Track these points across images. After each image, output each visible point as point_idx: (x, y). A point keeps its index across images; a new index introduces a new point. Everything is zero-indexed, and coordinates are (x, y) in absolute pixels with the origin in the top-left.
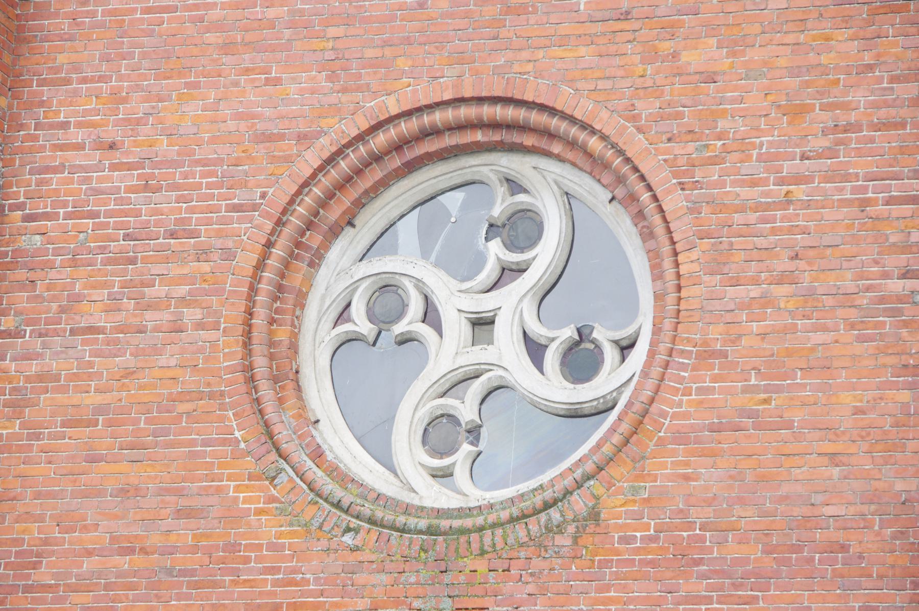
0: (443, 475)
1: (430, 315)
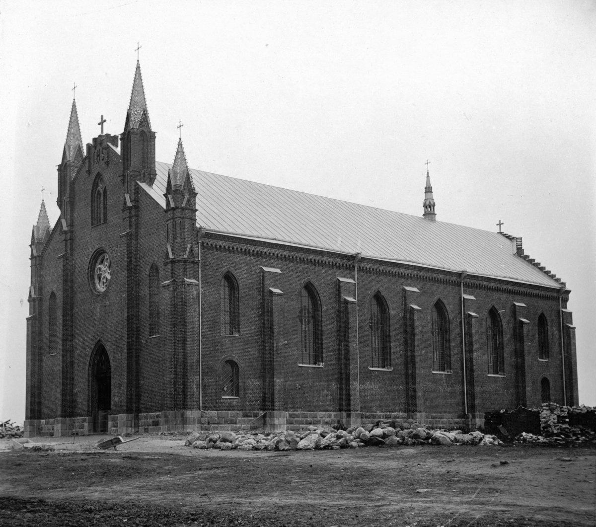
0: (103, 288)
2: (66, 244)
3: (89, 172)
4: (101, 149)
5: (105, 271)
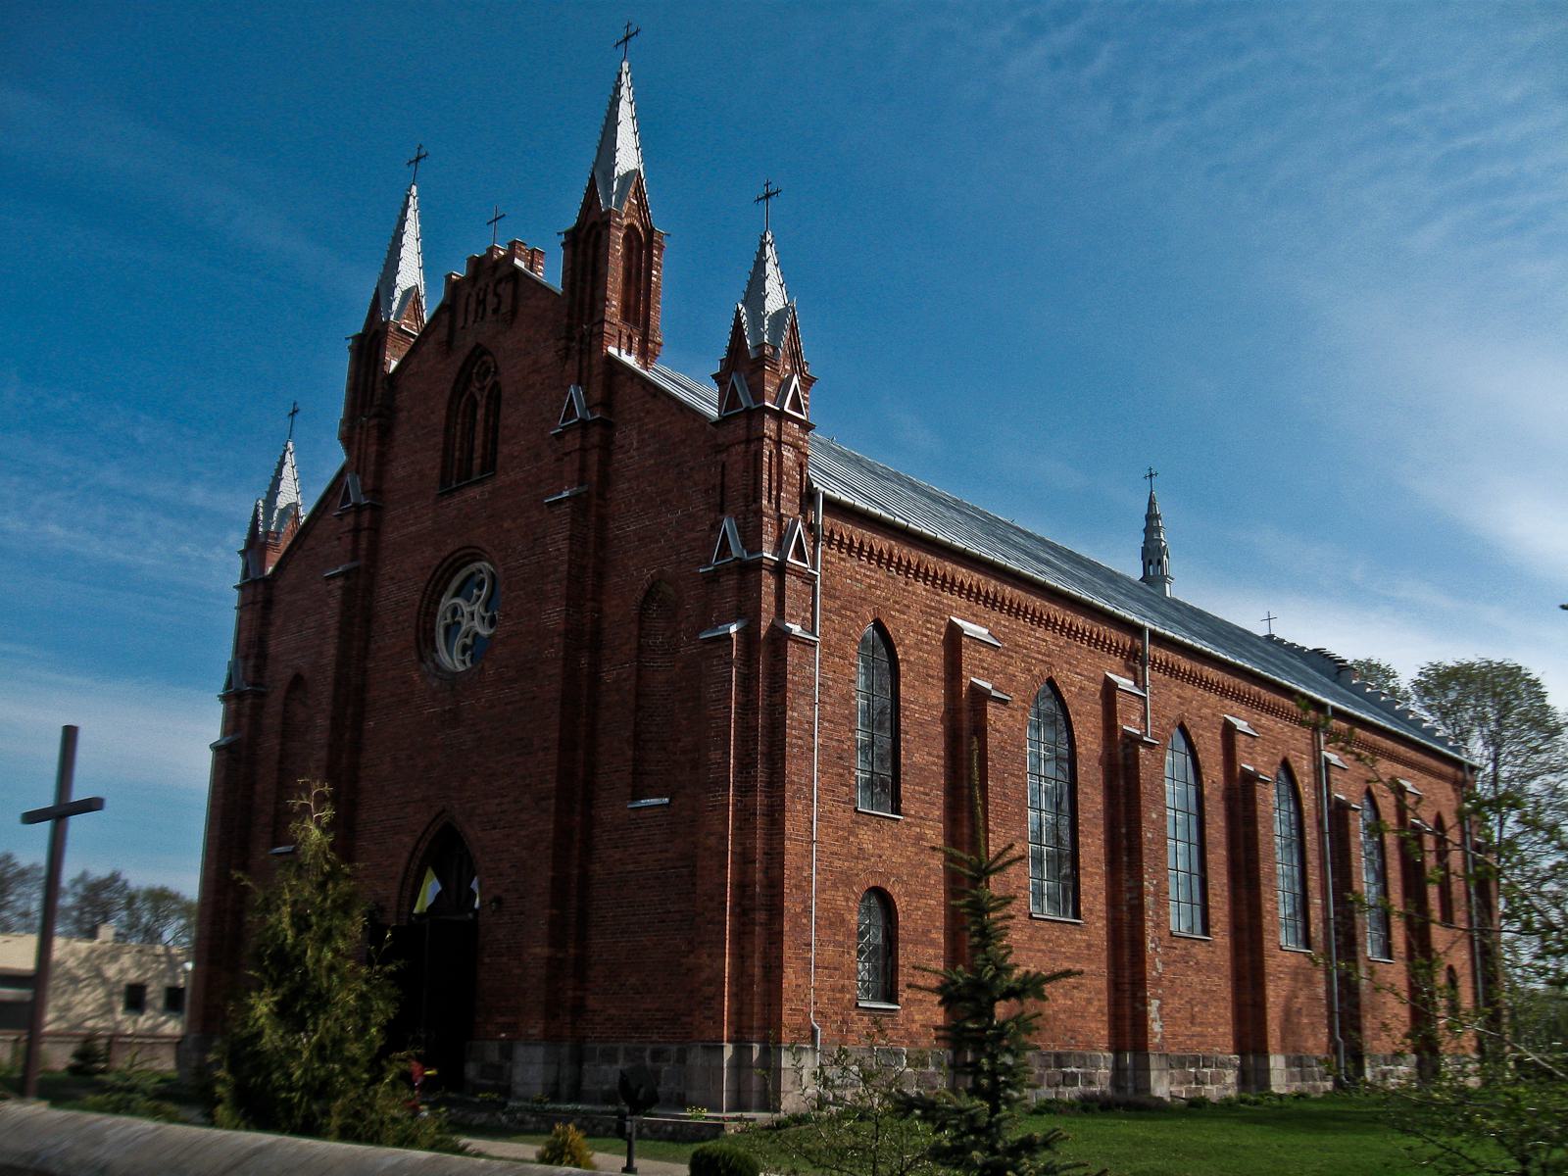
0: (464, 662)
1: (463, 615)
2: (356, 541)
3: (449, 345)
4: (491, 285)
5: (472, 614)
